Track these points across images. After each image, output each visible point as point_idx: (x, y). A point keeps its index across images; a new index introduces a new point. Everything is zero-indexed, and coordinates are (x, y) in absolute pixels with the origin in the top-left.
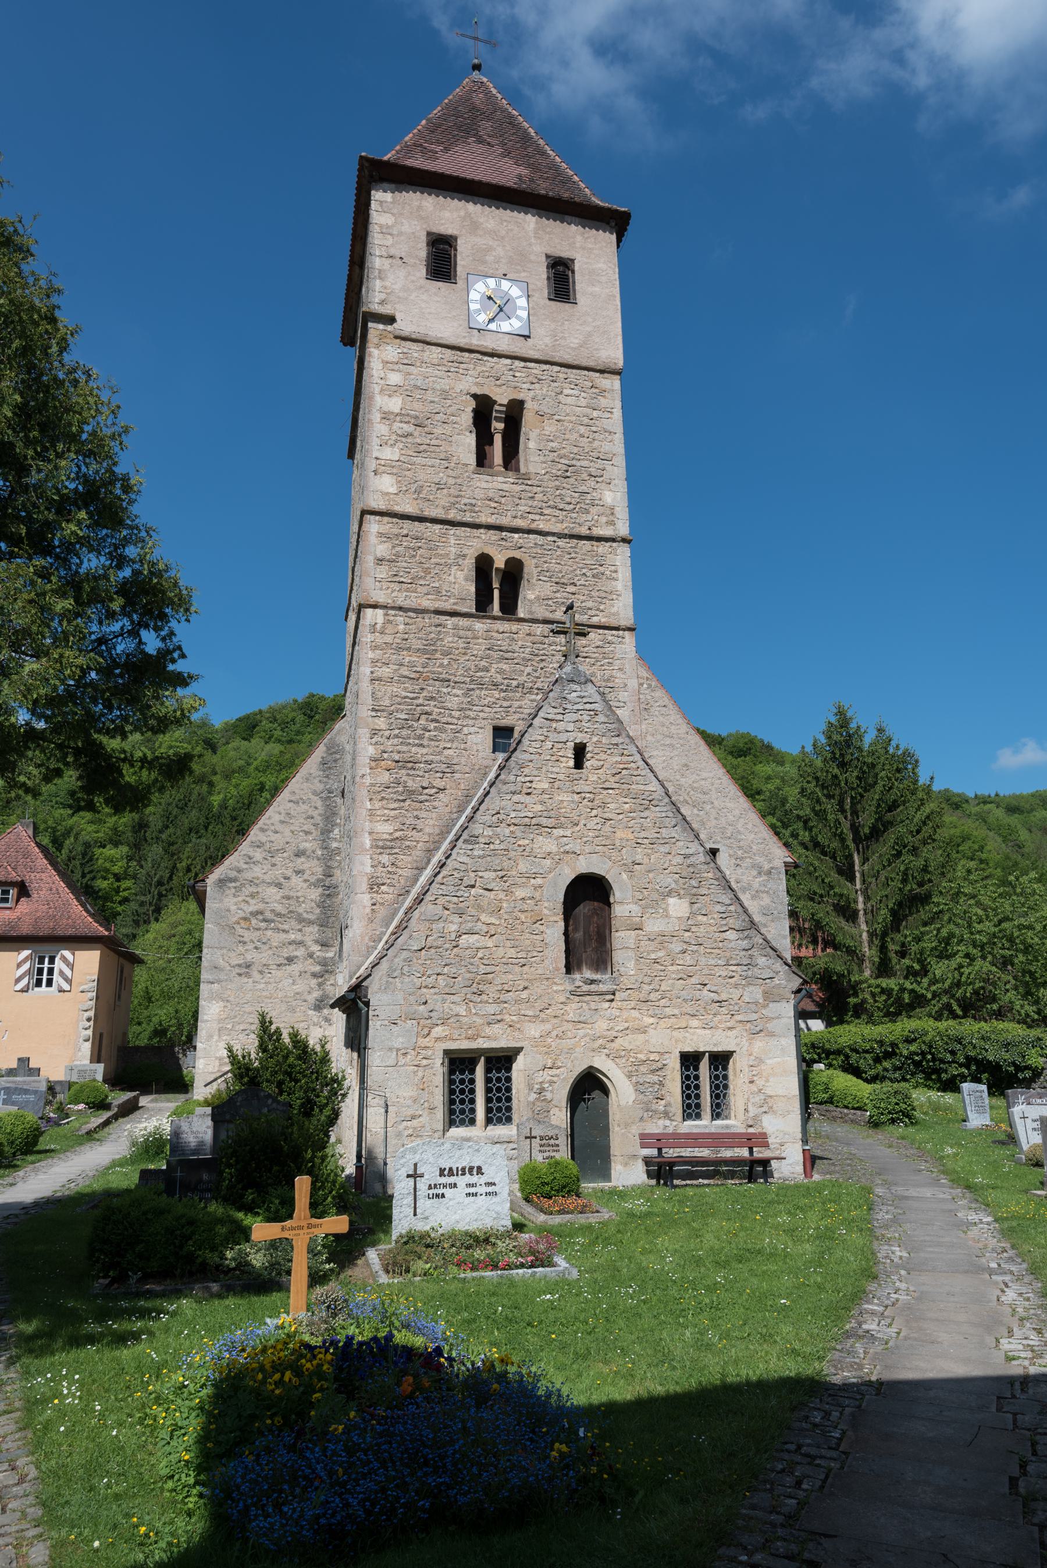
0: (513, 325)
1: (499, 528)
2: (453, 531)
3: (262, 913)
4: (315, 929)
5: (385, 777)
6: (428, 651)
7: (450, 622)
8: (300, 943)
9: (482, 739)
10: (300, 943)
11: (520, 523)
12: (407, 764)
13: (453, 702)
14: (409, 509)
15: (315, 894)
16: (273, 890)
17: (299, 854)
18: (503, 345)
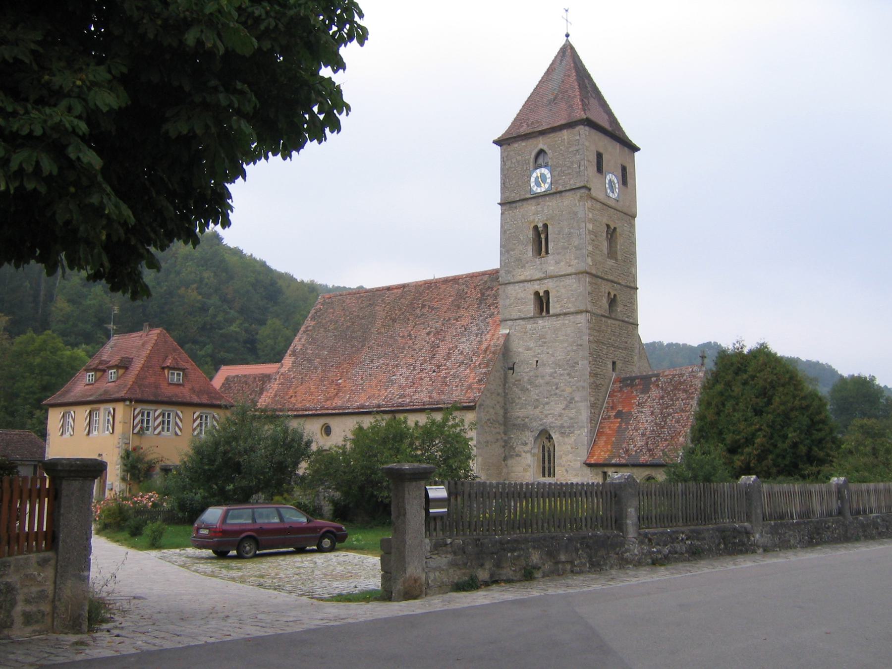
0: (614, 196)
1: (612, 281)
2: (604, 282)
3: (489, 420)
4: (502, 427)
5: (592, 380)
6: (599, 331)
7: (604, 319)
8: (499, 433)
9: (610, 366)
10: (499, 433)
11: (616, 280)
12: (596, 375)
13: (605, 351)
14: (594, 272)
15: (501, 412)
16: (491, 410)
17: (498, 395)
18: (612, 203)
